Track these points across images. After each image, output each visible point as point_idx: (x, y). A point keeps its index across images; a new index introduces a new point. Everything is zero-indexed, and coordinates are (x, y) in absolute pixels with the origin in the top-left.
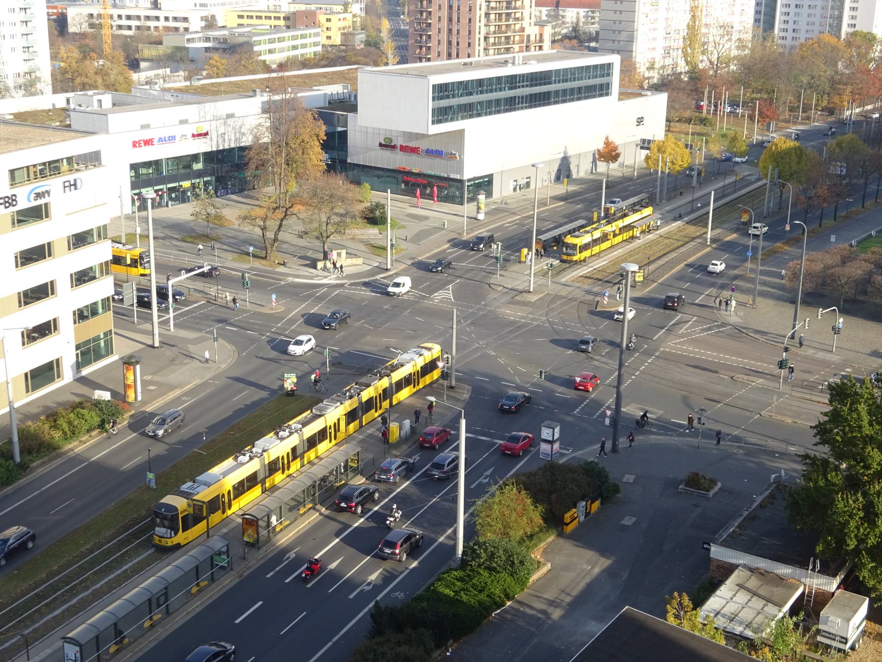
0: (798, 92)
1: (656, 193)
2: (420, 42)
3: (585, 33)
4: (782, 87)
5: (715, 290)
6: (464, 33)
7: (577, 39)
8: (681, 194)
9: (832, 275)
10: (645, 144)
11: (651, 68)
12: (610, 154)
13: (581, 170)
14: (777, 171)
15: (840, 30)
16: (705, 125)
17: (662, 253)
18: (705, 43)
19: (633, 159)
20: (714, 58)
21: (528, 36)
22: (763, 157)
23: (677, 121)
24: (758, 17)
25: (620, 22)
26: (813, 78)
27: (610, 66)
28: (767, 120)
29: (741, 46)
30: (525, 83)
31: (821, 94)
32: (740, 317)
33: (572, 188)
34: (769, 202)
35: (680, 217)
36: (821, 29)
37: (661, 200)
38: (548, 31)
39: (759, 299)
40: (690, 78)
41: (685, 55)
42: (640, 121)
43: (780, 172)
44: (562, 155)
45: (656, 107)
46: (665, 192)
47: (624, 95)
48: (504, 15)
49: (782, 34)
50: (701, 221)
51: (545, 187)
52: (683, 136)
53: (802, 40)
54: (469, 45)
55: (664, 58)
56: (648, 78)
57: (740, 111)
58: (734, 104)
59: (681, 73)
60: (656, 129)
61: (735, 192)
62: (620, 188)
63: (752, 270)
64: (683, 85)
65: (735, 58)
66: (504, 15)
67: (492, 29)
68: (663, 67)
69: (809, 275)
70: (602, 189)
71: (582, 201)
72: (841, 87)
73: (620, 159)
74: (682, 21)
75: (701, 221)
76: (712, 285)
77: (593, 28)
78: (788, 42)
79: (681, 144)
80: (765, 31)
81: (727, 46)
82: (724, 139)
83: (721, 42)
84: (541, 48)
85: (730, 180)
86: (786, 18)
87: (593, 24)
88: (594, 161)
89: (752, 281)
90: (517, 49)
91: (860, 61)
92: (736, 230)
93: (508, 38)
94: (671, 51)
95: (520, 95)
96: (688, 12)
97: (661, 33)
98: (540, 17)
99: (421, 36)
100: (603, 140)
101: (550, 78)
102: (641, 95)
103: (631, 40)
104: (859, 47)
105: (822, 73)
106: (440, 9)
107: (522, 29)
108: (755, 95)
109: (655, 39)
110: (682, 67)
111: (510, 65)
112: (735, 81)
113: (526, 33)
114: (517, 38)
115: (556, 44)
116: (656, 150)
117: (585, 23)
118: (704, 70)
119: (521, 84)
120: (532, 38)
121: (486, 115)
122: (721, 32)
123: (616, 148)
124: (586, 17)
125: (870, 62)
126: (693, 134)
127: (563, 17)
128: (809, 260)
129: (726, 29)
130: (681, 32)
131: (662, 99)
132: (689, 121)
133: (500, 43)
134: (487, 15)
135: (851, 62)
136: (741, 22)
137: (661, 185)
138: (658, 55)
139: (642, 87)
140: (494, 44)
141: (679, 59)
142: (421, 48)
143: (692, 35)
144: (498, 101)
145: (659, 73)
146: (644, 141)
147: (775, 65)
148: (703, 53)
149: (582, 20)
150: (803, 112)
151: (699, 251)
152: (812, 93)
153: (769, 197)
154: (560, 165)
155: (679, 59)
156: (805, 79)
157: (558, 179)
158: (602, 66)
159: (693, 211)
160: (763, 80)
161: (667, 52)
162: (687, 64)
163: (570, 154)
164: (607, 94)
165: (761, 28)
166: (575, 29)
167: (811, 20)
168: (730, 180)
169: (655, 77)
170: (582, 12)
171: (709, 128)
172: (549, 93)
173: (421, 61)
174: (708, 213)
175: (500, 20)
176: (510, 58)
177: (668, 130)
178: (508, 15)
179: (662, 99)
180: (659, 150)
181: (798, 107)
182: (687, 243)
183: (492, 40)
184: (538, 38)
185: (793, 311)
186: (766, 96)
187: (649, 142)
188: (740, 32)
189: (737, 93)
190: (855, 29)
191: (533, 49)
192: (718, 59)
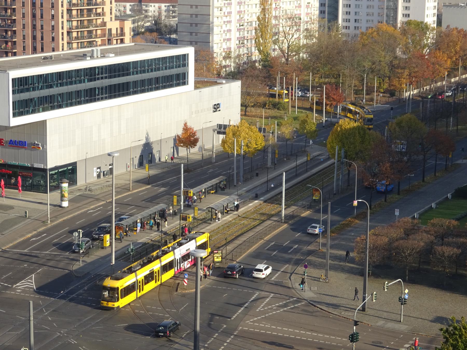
0: (362, 76)
1: (233, 175)
2: (5, 37)
3: (166, 26)
4: (347, 72)
5: (290, 266)
6: (47, 28)
7: (159, 33)
8: (257, 175)
9: (397, 248)
10: (221, 129)
11: (228, 56)
12: (188, 139)
13: (164, 154)
14: (342, 151)
15: (395, 18)
16: (278, 109)
17: (239, 233)
18: (276, 34)
19: (211, 143)
20: (285, 46)
21: (110, 30)
22: (330, 139)
23: (253, 106)
24: (323, 9)
25: (197, 15)
26: (374, 63)
27: (185, 57)
28: (334, 103)
29: (309, 34)
30: (104, 75)
31: (382, 77)
32: (313, 292)
33: (153, 172)
34: (337, 180)
35: (256, 197)
36: (380, 19)
37: (238, 181)
38: (128, 25)
39: (331, 273)
40: (264, 66)
41: (258, 45)
42: (216, 107)
43: (346, 152)
44: (143, 142)
45: (231, 93)
46: (241, 174)
47: (199, 85)
48: (85, 11)
49: (345, 24)
50: (276, 200)
51: (126, 171)
52: (258, 120)
53: (364, 30)
54: (53, 39)
55: (239, 47)
56: (225, 67)
57: (310, 95)
58: (304, 88)
59: (255, 61)
60: (232, 114)
61: (307, 171)
62: (197, 172)
63: (324, 245)
64: (257, 72)
65: (304, 46)
66: (85, 11)
67: (75, 24)
68: (239, 56)
69: (375, 248)
70: (180, 174)
71: (163, 185)
72: (400, 71)
73: (199, 144)
74: (253, 12)
75: (276, 200)
76: (288, 261)
77: (173, 22)
78: (352, 31)
79: (255, 129)
80: (329, 21)
81: (295, 36)
82: (296, 121)
83: (291, 32)
84: (122, 41)
85: (301, 160)
86: (348, 9)
87: (174, 17)
88: (176, 147)
89: (323, 256)
90: (99, 43)
91: (415, 47)
92: (309, 207)
93: (90, 32)
94: (245, 42)
95: (100, 86)
96: (258, 6)
97: (234, 26)
98: (125, 12)
99: (6, 31)
100: (182, 126)
101: (128, 70)
102: (216, 83)
103: (208, 33)
104: (413, 35)
105: (382, 59)
106: (23, 6)
107: (104, 24)
108: (323, 80)
109: (229, 31)
110: (256, 56)
111: (88, 58)
112: (304, 67)
113: (108, 26)
114: (99, 32)
115: (138, 37)
116: (231, 134)
117: (168, 17)
118: (276, 58)
119: (100, 76)
120: (114, 32)
121: (67, 106)
122: (289, 23)
123: (194, 134)
124: (168, 11)
125: (424, 48)
126: (266, 118)
127: (146, 11)
128: (373, 235)
129: (294, 20)
130: (254, 23)
131: (236, 86)
132: (264, 105)
133: (83, 37)
134: (69, 11)
135: (407, 48)
136: (307, 14)
137: (238, 168)
138: (233, 44)
139: (219, 75)
140: (77, 38)
141: (253, 49)
142: (6, 43)
143: (263, 26)
144: (78, 93)
145: (235, 62)
146: (220, 126)
147: (340, 53)
148: (275, 42)
149: (164, 14)
150: (367, 94)
151: (275, 229)
152: (374, 76)
153: (338, 175)
154: (143, 151)
155: (253, 49)
156: (367, 64)
157: (141, 164)
158: (178, 57)
159: (267, 191)
160: (330, 66)
161: (241, 41)
162: (260, 53)
163: (152, 140)
164: (184, 84)
165: (326, 19)
166: (157, 22)
167: (370, 11)
168: (301, 160)
169: (231, 65)
170: (163, 6)
171: (282, 112)
172: (128, 83)
173: (7, 56)
174: (281, 193)
175: (82, 15)
176: (88, 52)
177: (244, 114)
178: (90, 11)
179: (236, 86)
180: (234, 134)
181: (363, 90)
182: (264, 221)
183: (75, 34)
184: (119, 32)
185: (362, 283)
186: (333, 80)
187: (225, 126)
188: (307, 22)
189: (306, 78)
190: (409, 19)
191: (115, 42)
192: (288, 47)
